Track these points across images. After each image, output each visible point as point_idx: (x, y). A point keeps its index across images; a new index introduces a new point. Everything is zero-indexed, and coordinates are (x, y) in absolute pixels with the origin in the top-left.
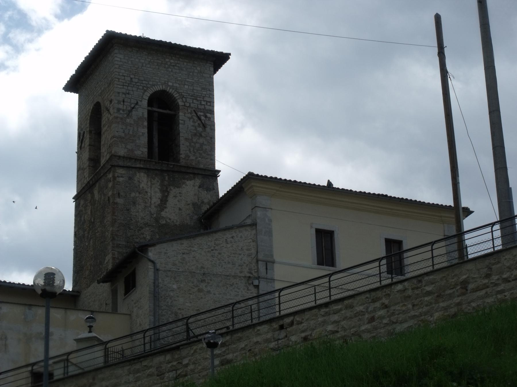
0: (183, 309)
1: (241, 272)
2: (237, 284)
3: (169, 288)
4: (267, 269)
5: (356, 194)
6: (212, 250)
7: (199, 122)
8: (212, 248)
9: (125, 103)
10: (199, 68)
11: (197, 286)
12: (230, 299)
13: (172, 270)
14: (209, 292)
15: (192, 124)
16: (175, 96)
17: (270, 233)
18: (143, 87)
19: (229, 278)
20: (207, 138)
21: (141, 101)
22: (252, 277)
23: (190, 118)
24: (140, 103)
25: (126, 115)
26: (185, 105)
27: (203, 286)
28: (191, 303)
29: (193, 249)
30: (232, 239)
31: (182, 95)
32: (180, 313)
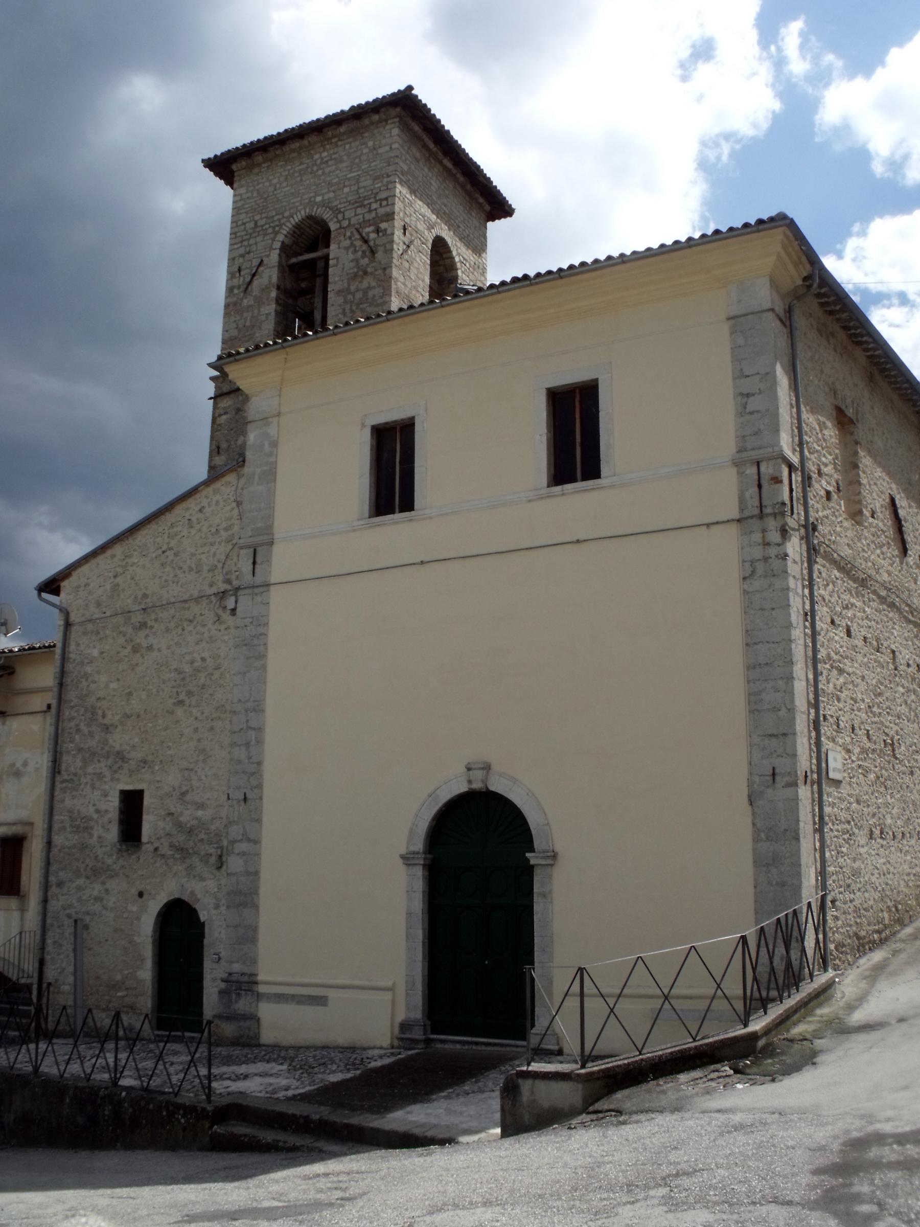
0: (104, 699)
1: (211, 585)
2: (201, 615)
3: (87, 658)
4: (254, 563)
5: (623, 262)
6: (164, 552)
7: (365, 247)
8: (164, 548)
9: (242, 273)
10: (370, 144)
11: (131, 641)
12: (185, 653)
13: (94, 618)
14: (150, 648)
15: (351, 256)
16: (290, 226)
17: (270, 475)
18: (274, 228)
19: (187, 606)
20: (377, 273)
21: (268, 256)
22: (230, 590)
23: (347, 249)
24: (266, 260)
25: (242, 294)
26: (341, 228)
27: (141, 638)
28: (118, 680)
29: (130, 561)
30: (200, 515)
31: (337, 209)
32: (100, 708)
